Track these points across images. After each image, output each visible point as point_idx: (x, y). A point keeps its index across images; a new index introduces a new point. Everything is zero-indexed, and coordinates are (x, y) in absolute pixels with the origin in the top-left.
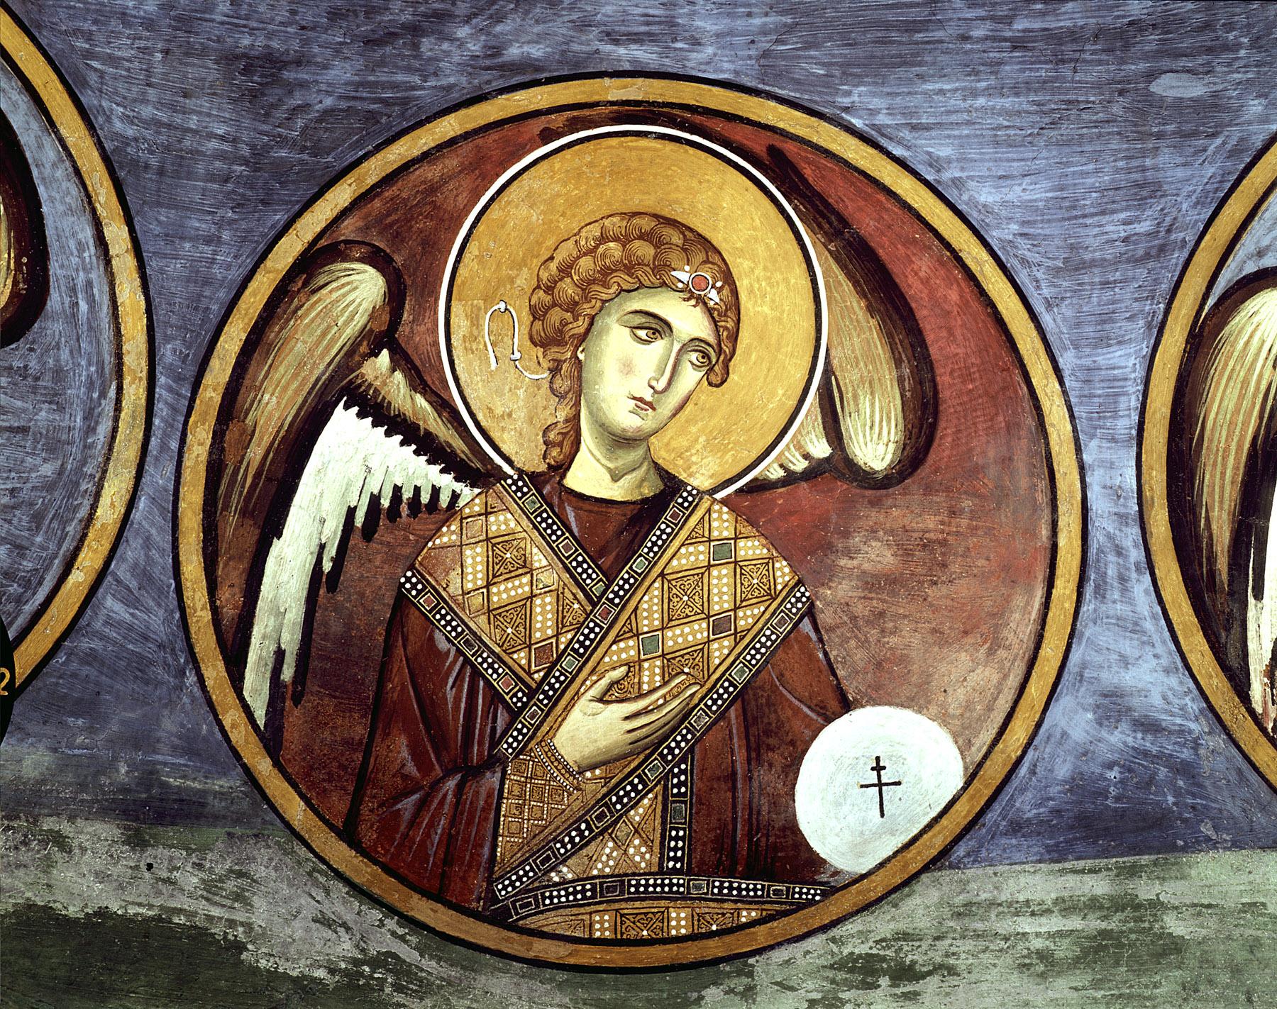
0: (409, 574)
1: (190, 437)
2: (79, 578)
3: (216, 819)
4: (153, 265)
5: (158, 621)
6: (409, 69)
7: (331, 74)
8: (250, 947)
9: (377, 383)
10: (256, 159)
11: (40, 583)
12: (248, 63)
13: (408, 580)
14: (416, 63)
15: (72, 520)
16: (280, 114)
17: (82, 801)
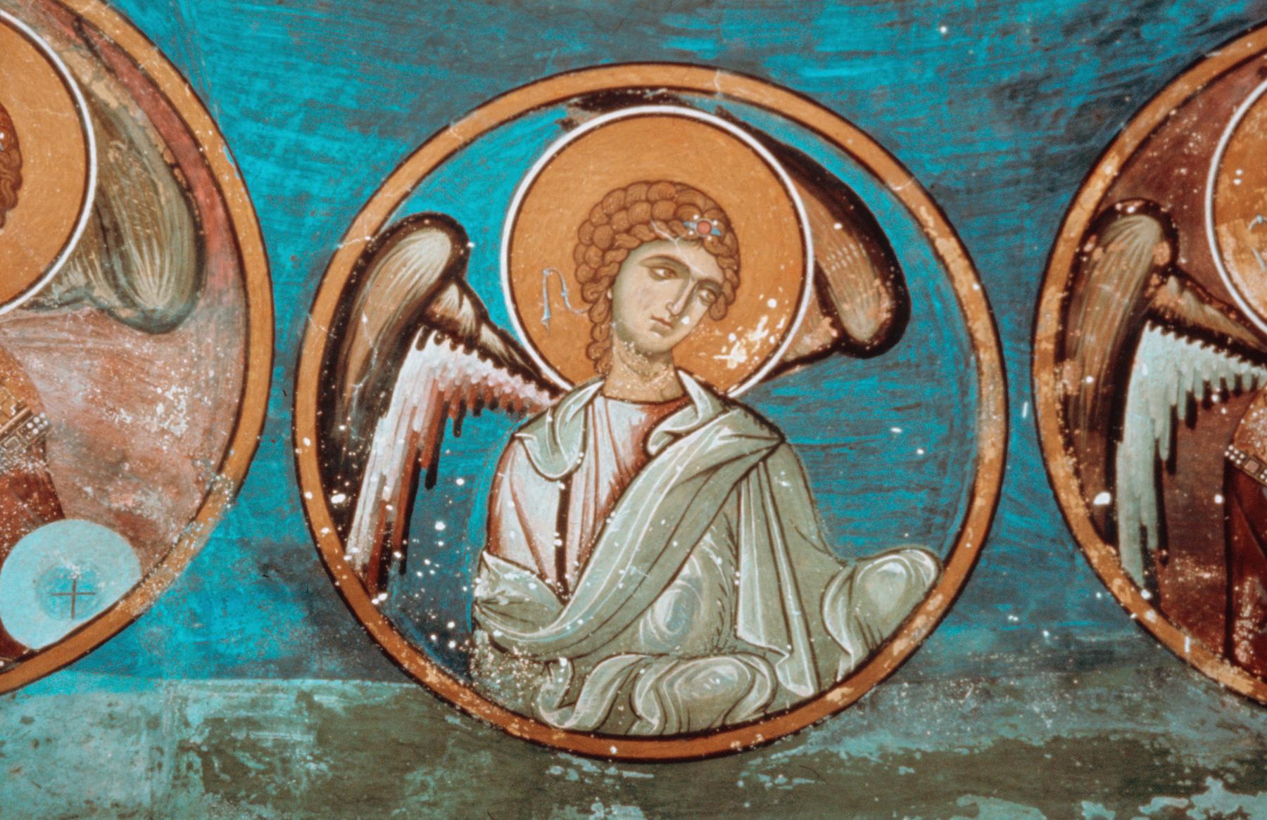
0: (1231, 448)
1: (1036, 381)
2: (981, 503)
3: (1124, 661)
4: (980, 261)
5: (1047, 523)
6: (1138, 54)
7: (1076, 79)
8: (1173, 751)
9: (1172, 305)
10: (1038, 154)
11: (955, 512)
12: (1013, 91)
13: (1232, 452)
14: (1143, 48)
15: (965, 462)
16: (1046, 121)
17: (1023, 664)
